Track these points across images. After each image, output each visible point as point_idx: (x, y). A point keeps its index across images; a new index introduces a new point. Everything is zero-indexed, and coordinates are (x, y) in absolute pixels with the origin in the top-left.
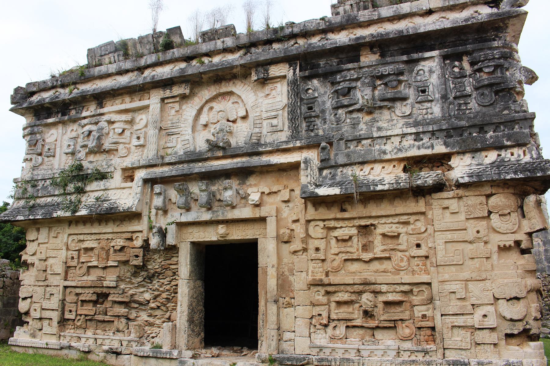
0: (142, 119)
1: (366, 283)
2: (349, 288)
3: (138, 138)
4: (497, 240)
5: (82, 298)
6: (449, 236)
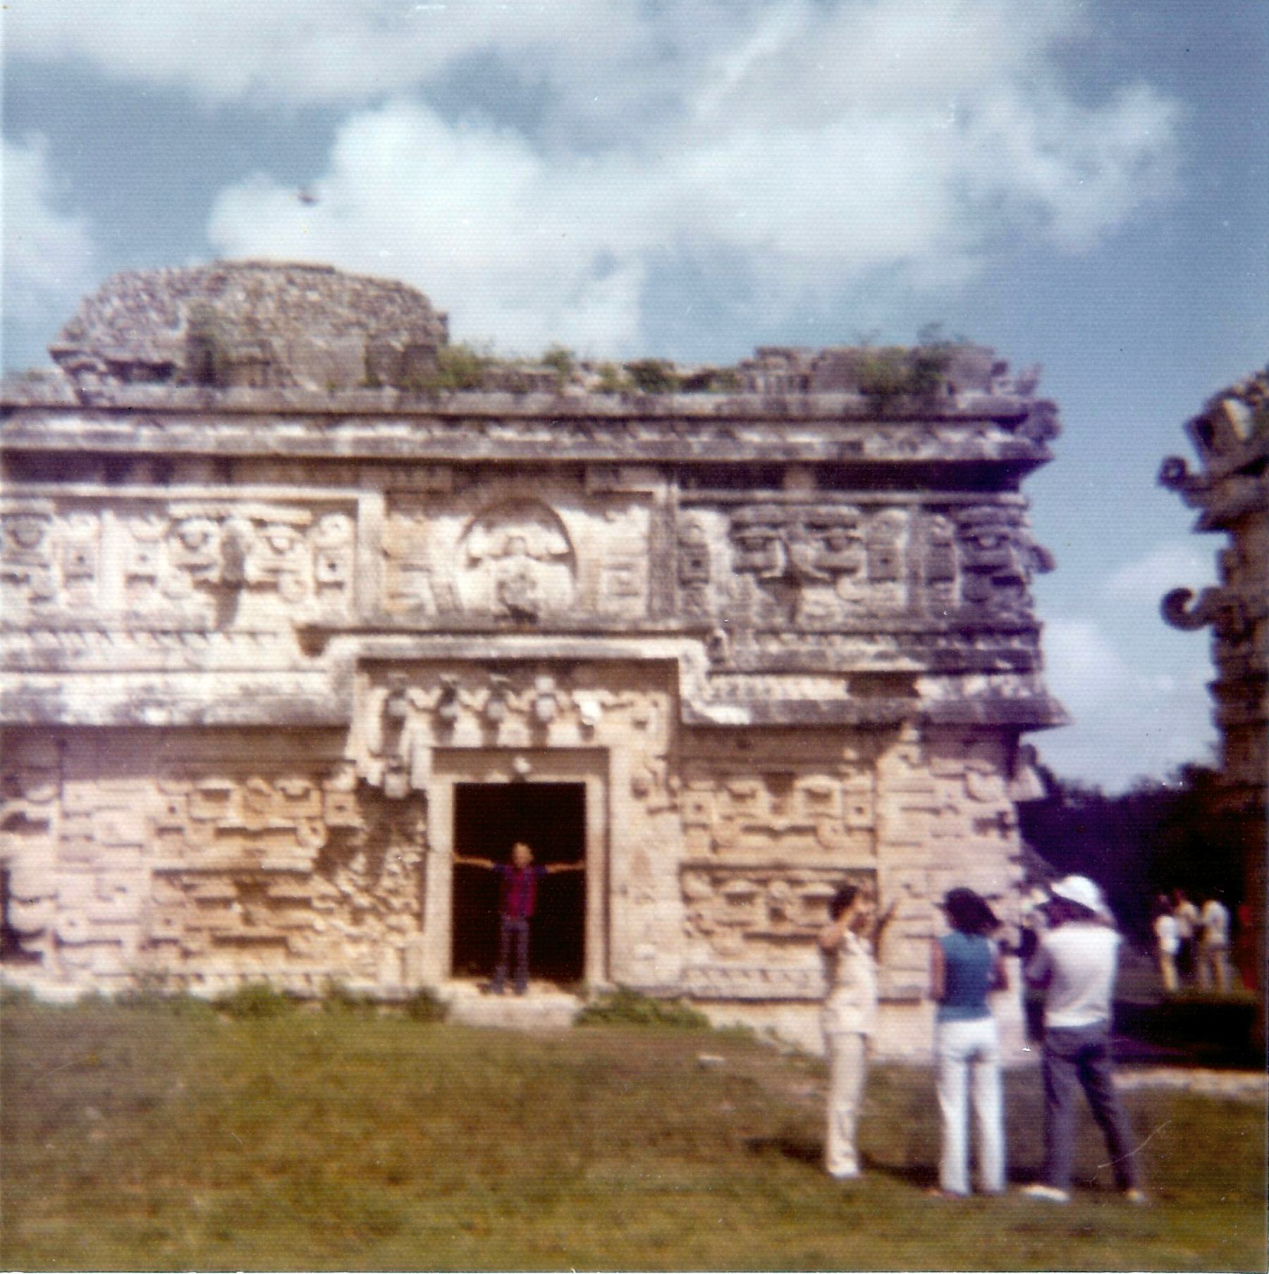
0: (336, 528)
1: (780, 867)
2: (751, 875)
3: (332, 566)
4: (971, 809)
5: (196, 894)
6: (907, 799)
